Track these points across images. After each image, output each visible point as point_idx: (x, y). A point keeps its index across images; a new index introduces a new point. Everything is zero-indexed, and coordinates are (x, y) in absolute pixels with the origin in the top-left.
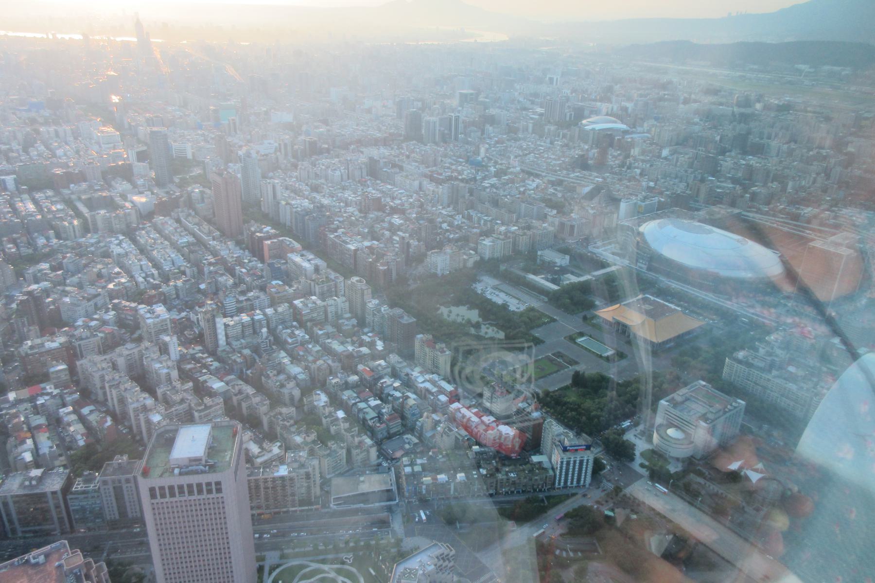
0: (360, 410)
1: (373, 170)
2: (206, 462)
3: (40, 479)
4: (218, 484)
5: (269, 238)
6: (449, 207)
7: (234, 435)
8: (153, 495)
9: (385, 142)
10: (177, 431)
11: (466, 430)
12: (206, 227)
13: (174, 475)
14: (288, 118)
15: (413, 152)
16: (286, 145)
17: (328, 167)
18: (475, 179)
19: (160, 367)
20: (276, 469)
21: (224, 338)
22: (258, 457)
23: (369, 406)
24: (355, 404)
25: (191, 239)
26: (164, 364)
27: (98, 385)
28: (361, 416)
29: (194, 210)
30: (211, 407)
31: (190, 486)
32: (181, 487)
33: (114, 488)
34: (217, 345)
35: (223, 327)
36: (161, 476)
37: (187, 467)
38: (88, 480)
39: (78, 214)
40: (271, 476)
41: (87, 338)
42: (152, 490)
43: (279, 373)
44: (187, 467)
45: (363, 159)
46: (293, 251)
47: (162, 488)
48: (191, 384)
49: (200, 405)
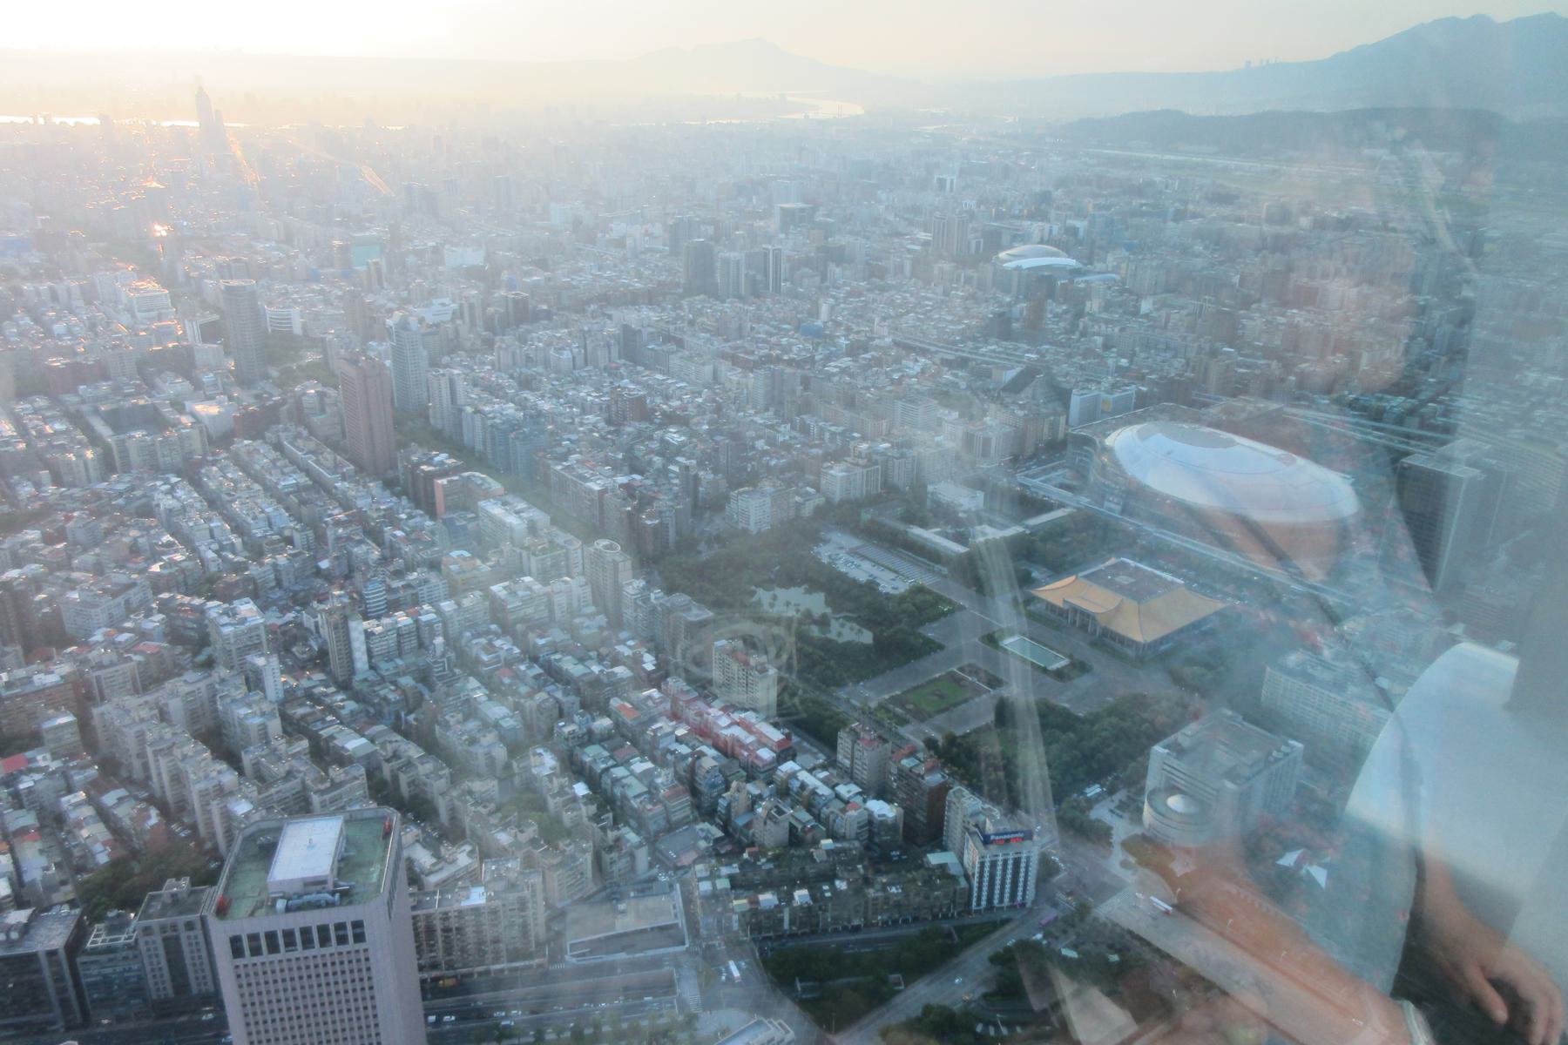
0: (616, 781)
1: (630, 346)
2: (336, 885)
3: (25, 929)
4: (358, 925)
5: (445, 474)
6: (767, 410)
7: (387, 834)
8: (237, 951)
9: (650, 298)
10: (278, 831)
12: (328, 456)
13: (275, 912)
14: (475, 257)
15: (700, 313)
16: (471, 307)
17: (549, 345)
18: (812, 360)
19: (249, 714)
20: (464, 893)
21: (365, 658)
22: (431, 873)
23: (632, 773)
24: (607, 770)
25: (303, 479)
26: (255, 708)
28: (618, 791)
29: (308, 427)
30: (341, 784)
31: (306, 932)
32: (289, 935)
33: (165, 940)
35: (362, 637)
36: (252, 914)
37: (300, 896)
38: (117, 927)
39: (94, 439)
40: (456, 907)
41: (112, 664)
42: (235, 942)
43: (467, 717)
44: (300, 896)
45: (611, 329)
46: (487, 495)
47: (254, 938)
48: (305, 743)
49: (322, 781)
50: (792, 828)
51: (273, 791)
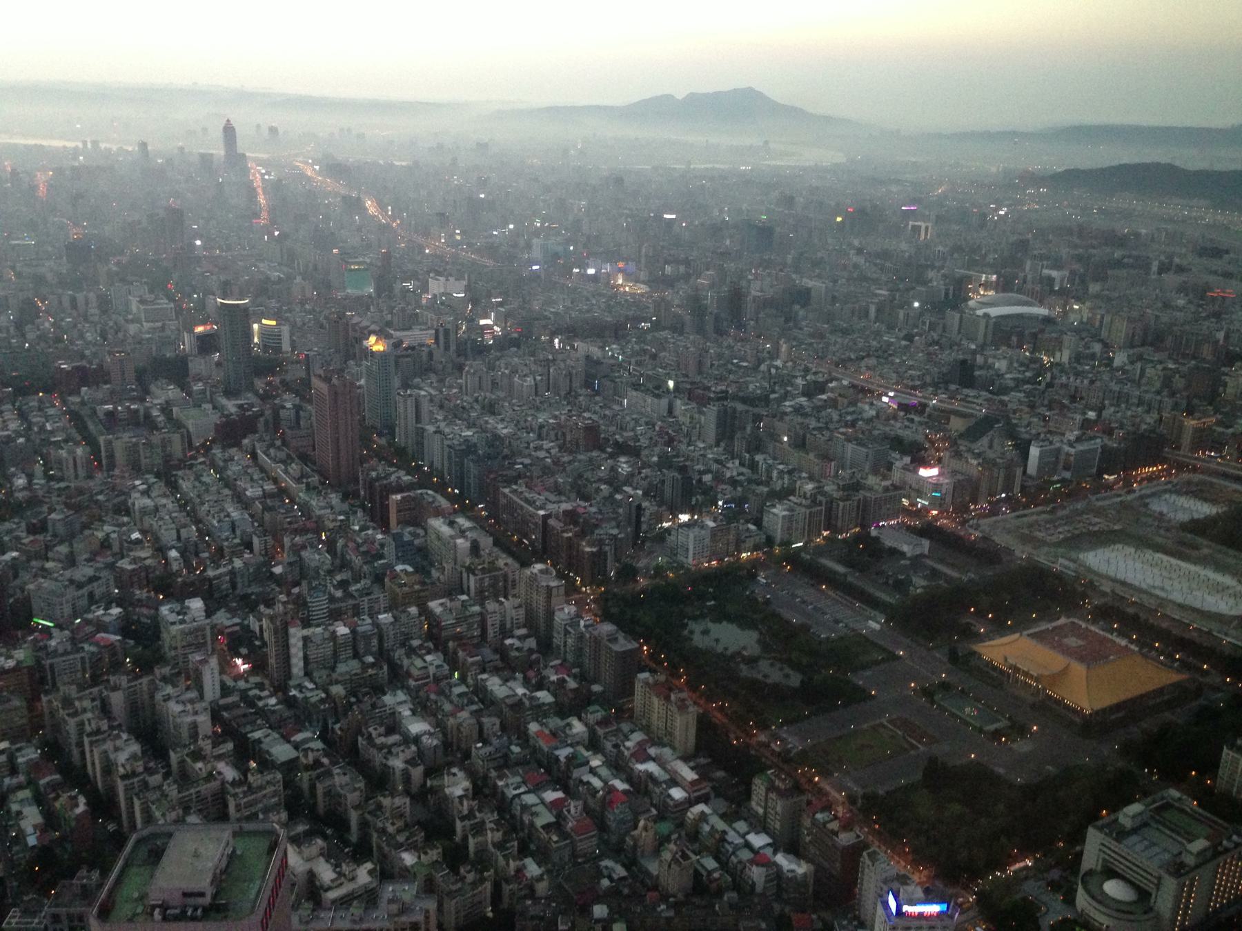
0: (525, 808)
6: (717, 445)
11: (716, 858)
19: (182, 711)
21: (301, 664)
22: (329, 889)
23: (543, 802)
24: (519, 795)
26: (189, 707)
27: (73, 738)
28: (526, 818)
34: (289, 676)
35: (300, 644)
39: (91, 442)
41: (66, 653)
43: (390, 730)
48: (230, 746)
50: (697, 874)
51: (192, 791)
